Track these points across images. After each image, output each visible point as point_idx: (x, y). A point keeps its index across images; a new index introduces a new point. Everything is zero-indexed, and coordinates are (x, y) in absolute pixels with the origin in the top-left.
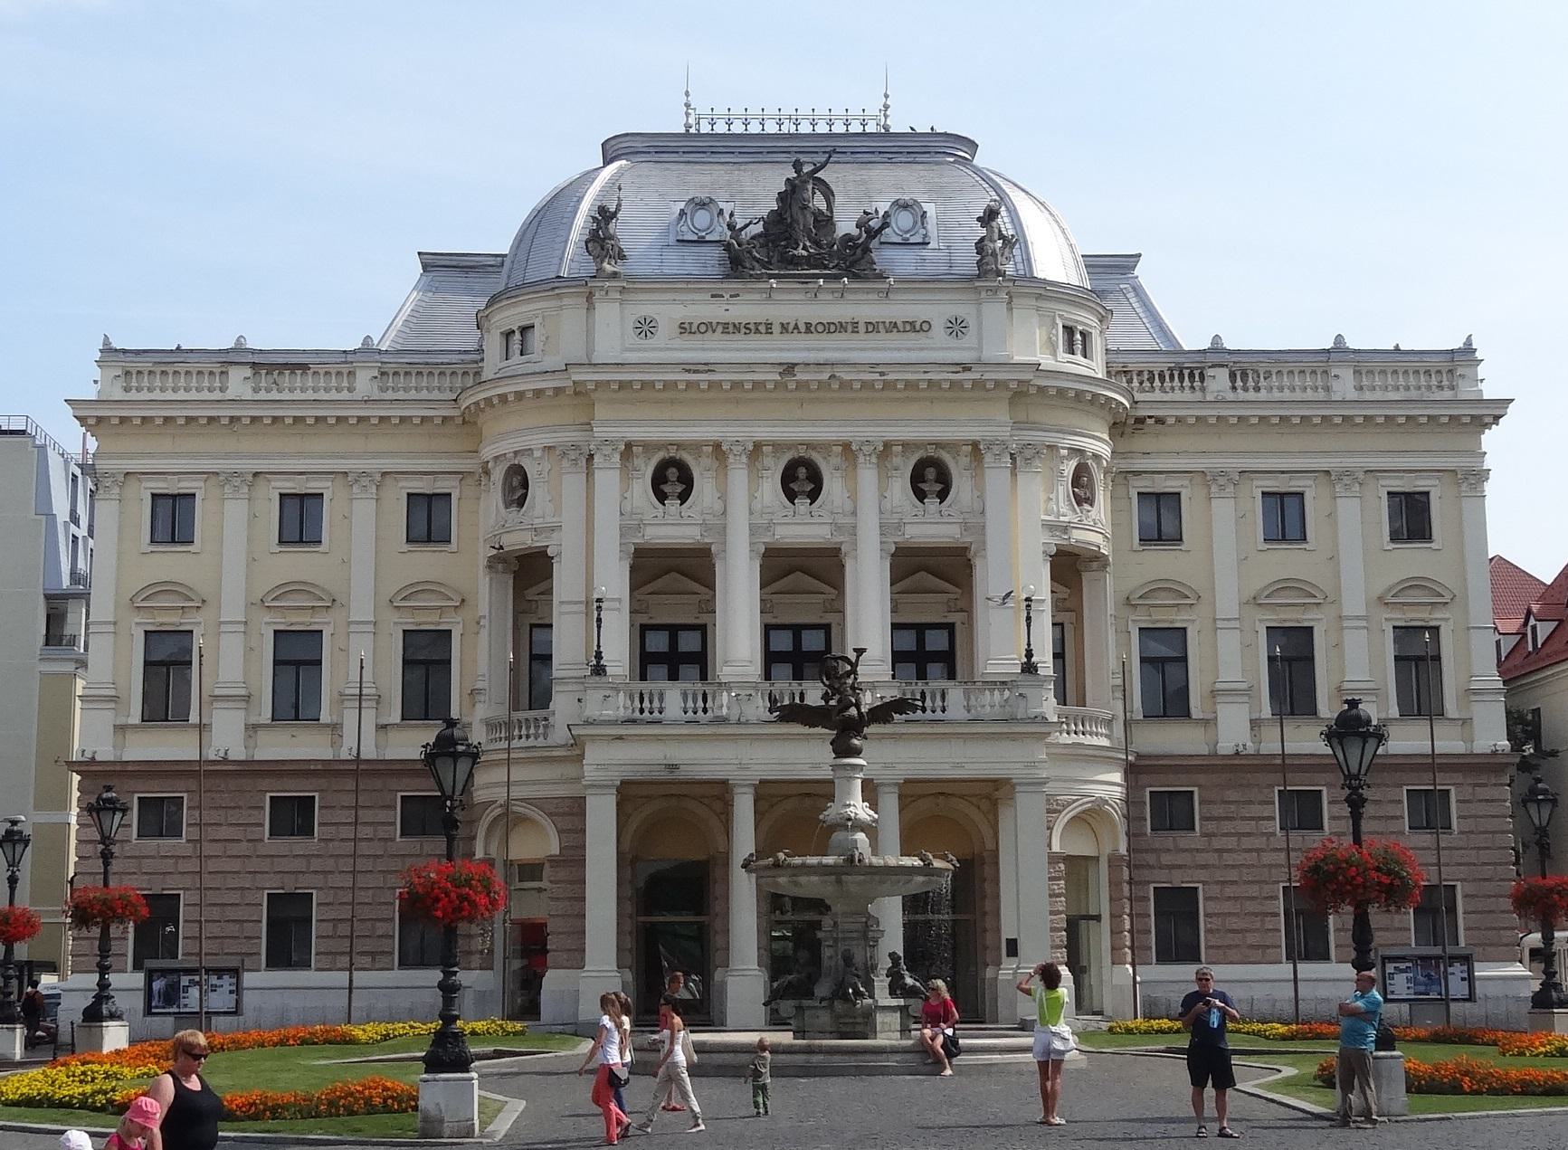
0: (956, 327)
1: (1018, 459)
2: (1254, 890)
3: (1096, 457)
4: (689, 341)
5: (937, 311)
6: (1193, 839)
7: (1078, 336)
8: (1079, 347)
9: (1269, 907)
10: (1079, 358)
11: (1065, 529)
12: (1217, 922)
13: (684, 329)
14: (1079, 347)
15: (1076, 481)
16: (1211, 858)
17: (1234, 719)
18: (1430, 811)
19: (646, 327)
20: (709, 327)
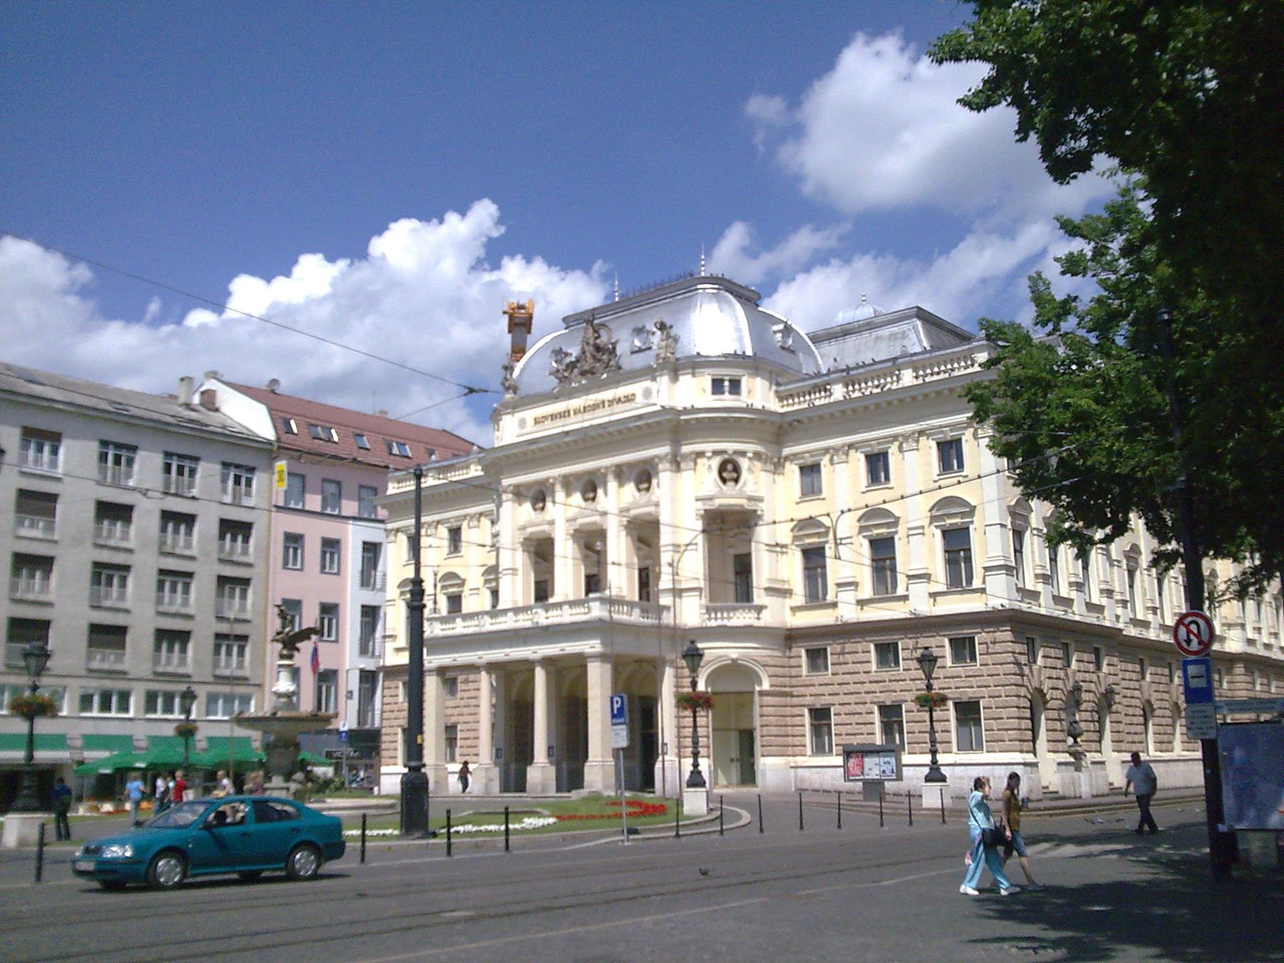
0: (647, 393)
1: (676, 463)
2: (860, 708)
3: (743, 454)
4: (540, 426)
5: (636, 388)
6: (827, 676)
7: (727, 383)
8: (727, 389)
9: (868, 718)
10: (727, 395)
11: (711, 499)
12: (843, 729)
13: (537, 421)
14: (727, 389)
15: (722, 468)
16: (836, 688)
17: (851, 596)
18: (964, 649)
19: (522, 423)
20: (545, 418)
